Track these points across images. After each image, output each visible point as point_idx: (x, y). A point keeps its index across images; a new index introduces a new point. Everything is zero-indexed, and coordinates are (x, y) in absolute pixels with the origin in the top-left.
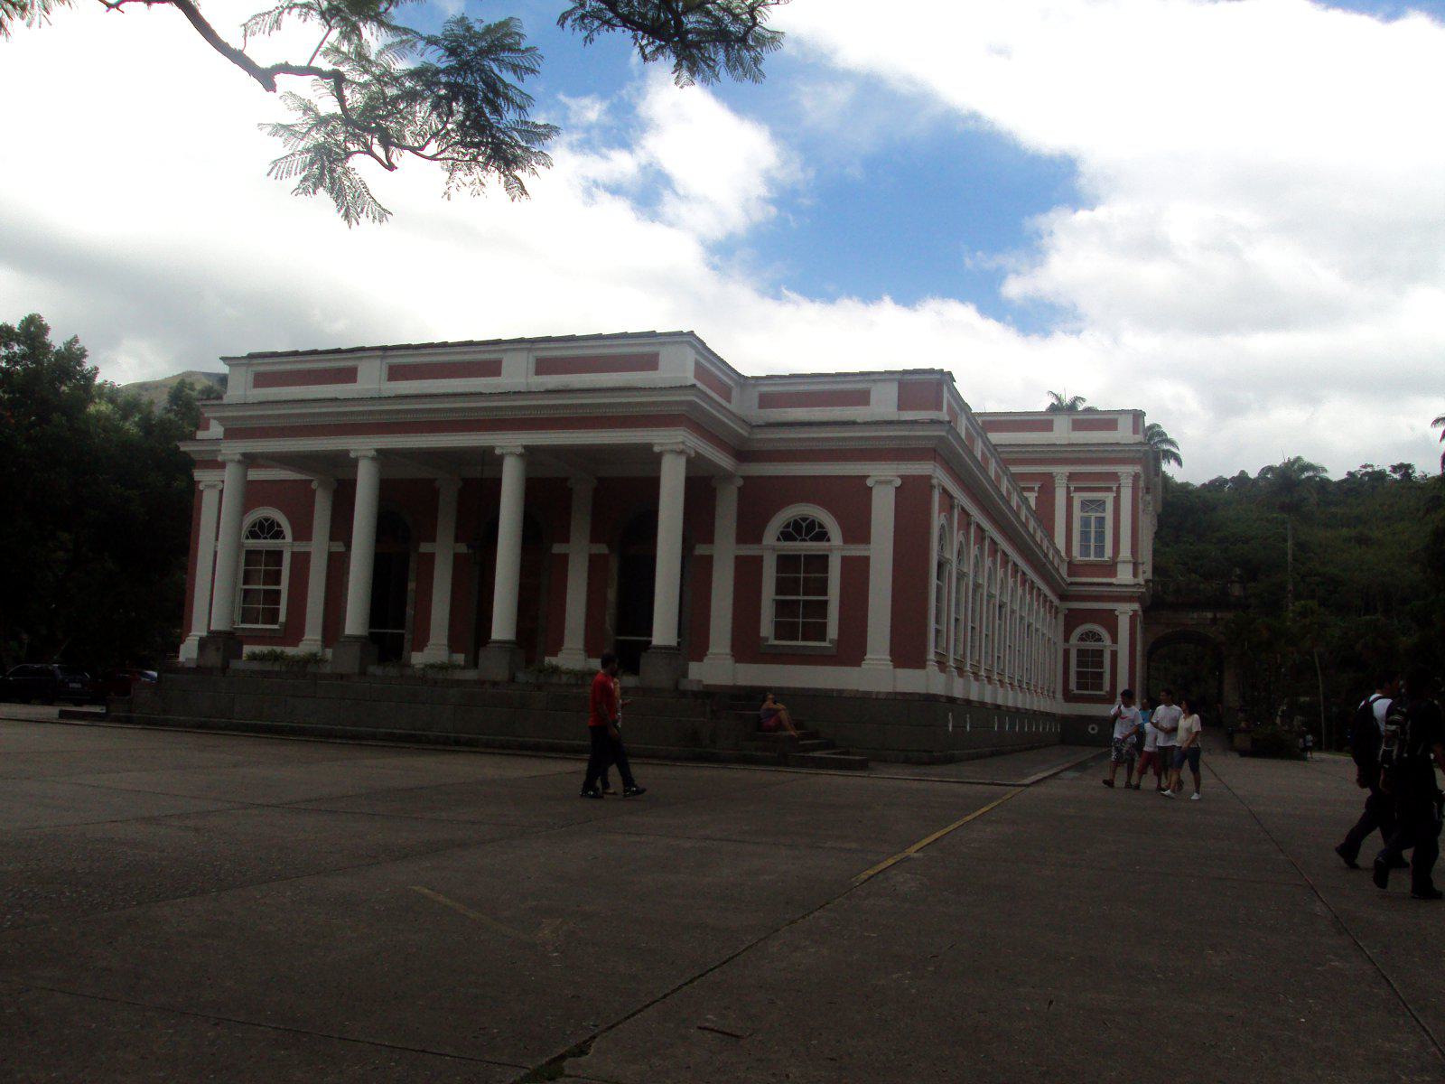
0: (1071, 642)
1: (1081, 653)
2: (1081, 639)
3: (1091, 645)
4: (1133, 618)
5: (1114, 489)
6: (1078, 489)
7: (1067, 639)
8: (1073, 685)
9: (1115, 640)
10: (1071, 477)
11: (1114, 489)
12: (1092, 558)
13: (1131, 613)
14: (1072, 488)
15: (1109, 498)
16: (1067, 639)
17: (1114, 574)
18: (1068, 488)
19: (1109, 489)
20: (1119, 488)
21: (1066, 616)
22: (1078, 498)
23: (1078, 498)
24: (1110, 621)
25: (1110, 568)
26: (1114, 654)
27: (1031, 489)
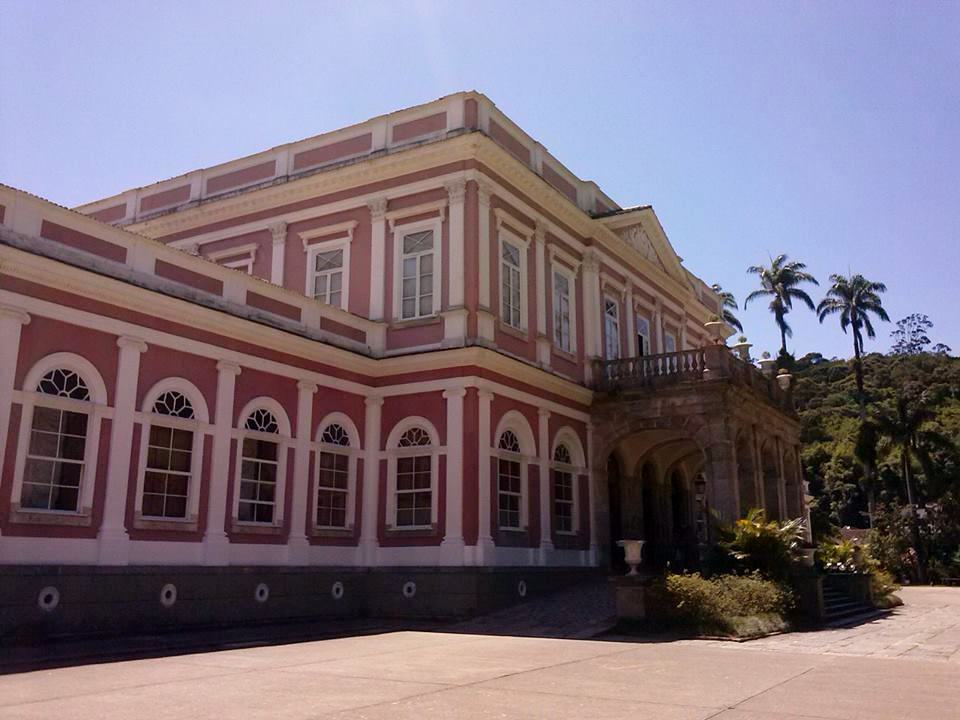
1: (403, 464)
2: (403, 443)
3: (415, 451)
6: (398, 222)
7: (383, 448)
8: (391, 518)
9: (443, 442)
10: (391, 205)
11: (442, 212)
14: (391, 223)
15: (435, 224)
16: (383, 448)
17: (441, 337)
18: (387, 222)
19: (435, 214)
20: (447, 209)
21: (384, 408)
22: (399, 232)
23: (399, 232)
24: (434, 407)
26: (443, 459)
27: (344, 234)
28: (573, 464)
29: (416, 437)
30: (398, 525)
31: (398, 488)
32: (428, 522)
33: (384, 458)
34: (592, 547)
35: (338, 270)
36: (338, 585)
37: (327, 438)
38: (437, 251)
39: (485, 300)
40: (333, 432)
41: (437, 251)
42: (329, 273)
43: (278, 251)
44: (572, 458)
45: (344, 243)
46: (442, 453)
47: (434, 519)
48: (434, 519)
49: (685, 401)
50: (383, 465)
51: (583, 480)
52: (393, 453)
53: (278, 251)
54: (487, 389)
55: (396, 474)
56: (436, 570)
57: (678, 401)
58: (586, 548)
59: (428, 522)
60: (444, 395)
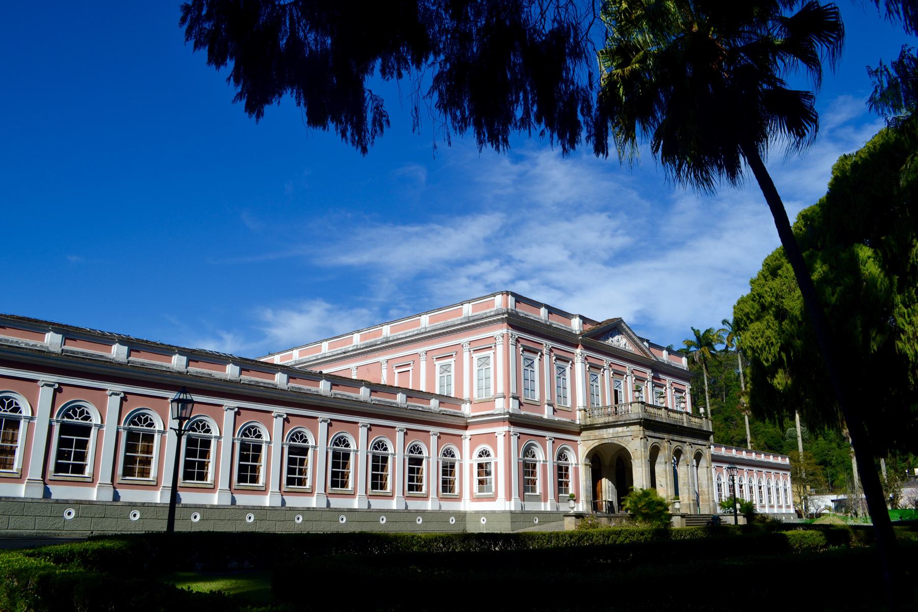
0: (473, 459)
2: (480, 456)
3: (484, 460)
4: (508, 436)
5: (493, 347)
7: (471, 457)
9: (496, 455)
10: (470, 343)
12: (484, 397)
13: (504, 434)
15: (489, 353)
16: (471, 457)
17: (493, 407)
22: (476, 356)
25: (491, 401)
26: (496, 463)
28: (570, 462)
29: (484, 453)
30: (479, 492)
31: (478, 476)
32: (491, 491)
33: (472, 462)
34: (581, 502)
35: (449, 374)
36: (453, 518)
37: (445, 455)
38: (492, 366)
39: (513, 390)
40: (447, 452)
41: (492, 366)
42: (445, 374)
43: (423, 365)
44: (569, 459)
45: (451, 361)
46: (496, 461)
47: (493, 490)
48: (493, 490)
49: (623, 430)
50: (471, 465)
51: (576, 470)
52: (476, 460)
53: (423, 365)
54: (512, 429)
55: (477, 470)
56: (493, 512)
57: (620, 429)
58: (546, 500)
59: (491, 491)
60: (496, 434)
